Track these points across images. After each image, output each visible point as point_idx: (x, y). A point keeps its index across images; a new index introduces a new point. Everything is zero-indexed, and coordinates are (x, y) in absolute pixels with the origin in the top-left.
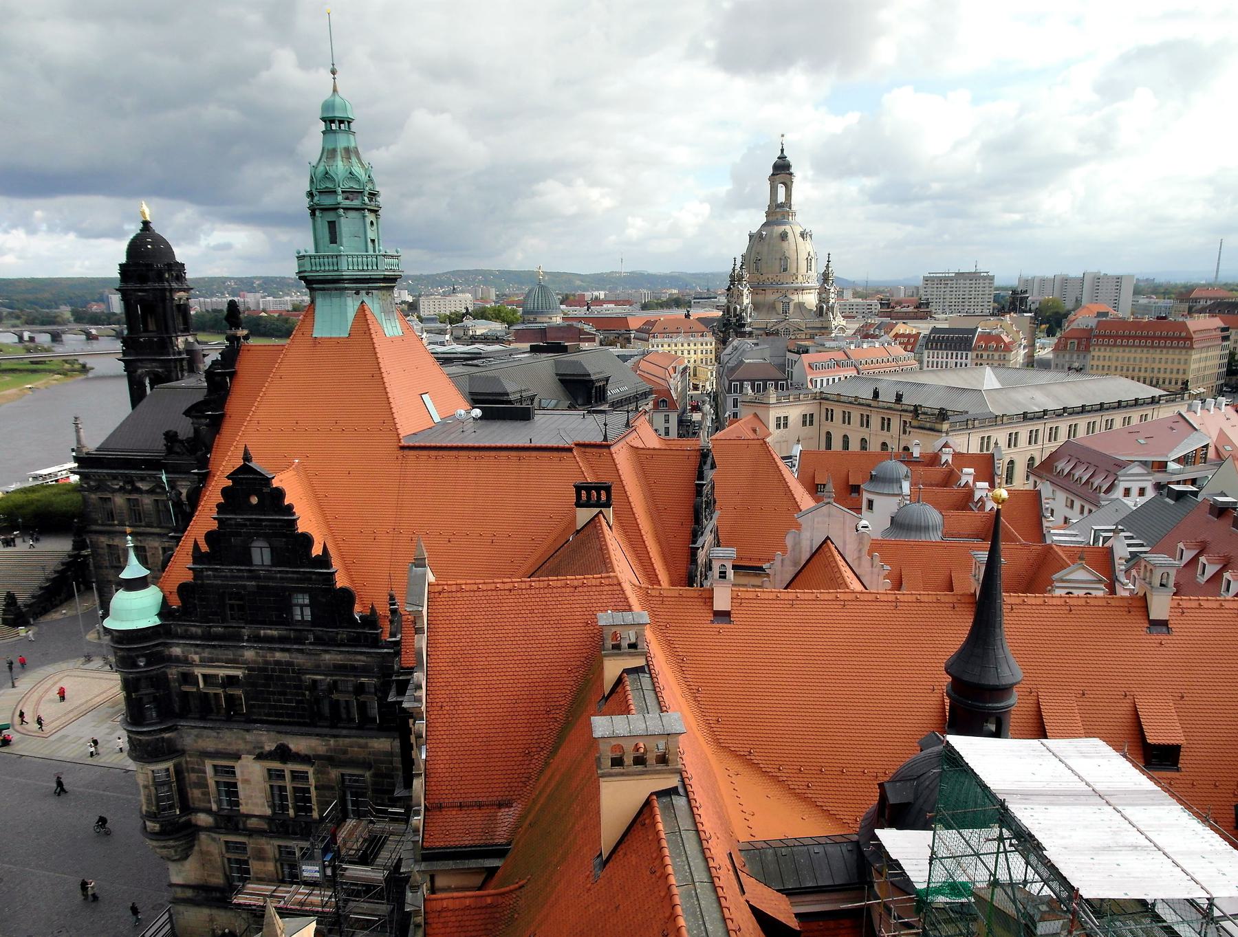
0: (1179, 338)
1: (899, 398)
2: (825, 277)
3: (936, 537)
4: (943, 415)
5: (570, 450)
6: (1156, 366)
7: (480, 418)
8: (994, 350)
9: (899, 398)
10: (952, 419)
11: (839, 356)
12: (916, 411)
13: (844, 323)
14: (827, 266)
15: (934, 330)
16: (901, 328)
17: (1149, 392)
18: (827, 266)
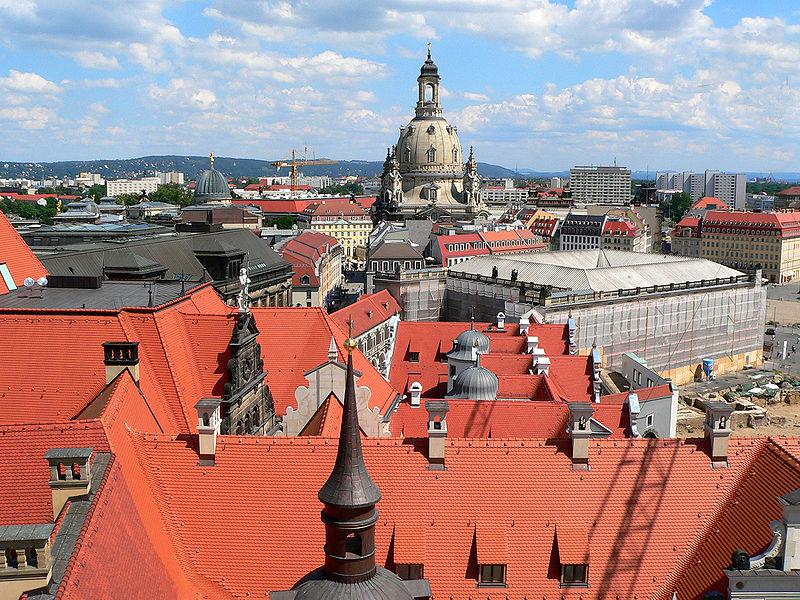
0: (771, 229)
1: (514, 275)
2: (469, 167)
3: (490, 397)
4: (545, 291)
5: (115, 314)
6: (754, 252)
7: (48, 286)
8: (621, 240)
9: (514, 275)
10: (554, 295)
11: (474, 239)
12: (523, 288)
13: (486, 209)
14: (470, 159)
15: (570, 217)
16: (541, 214)
17: (735, 273)
18: (470, 159)
